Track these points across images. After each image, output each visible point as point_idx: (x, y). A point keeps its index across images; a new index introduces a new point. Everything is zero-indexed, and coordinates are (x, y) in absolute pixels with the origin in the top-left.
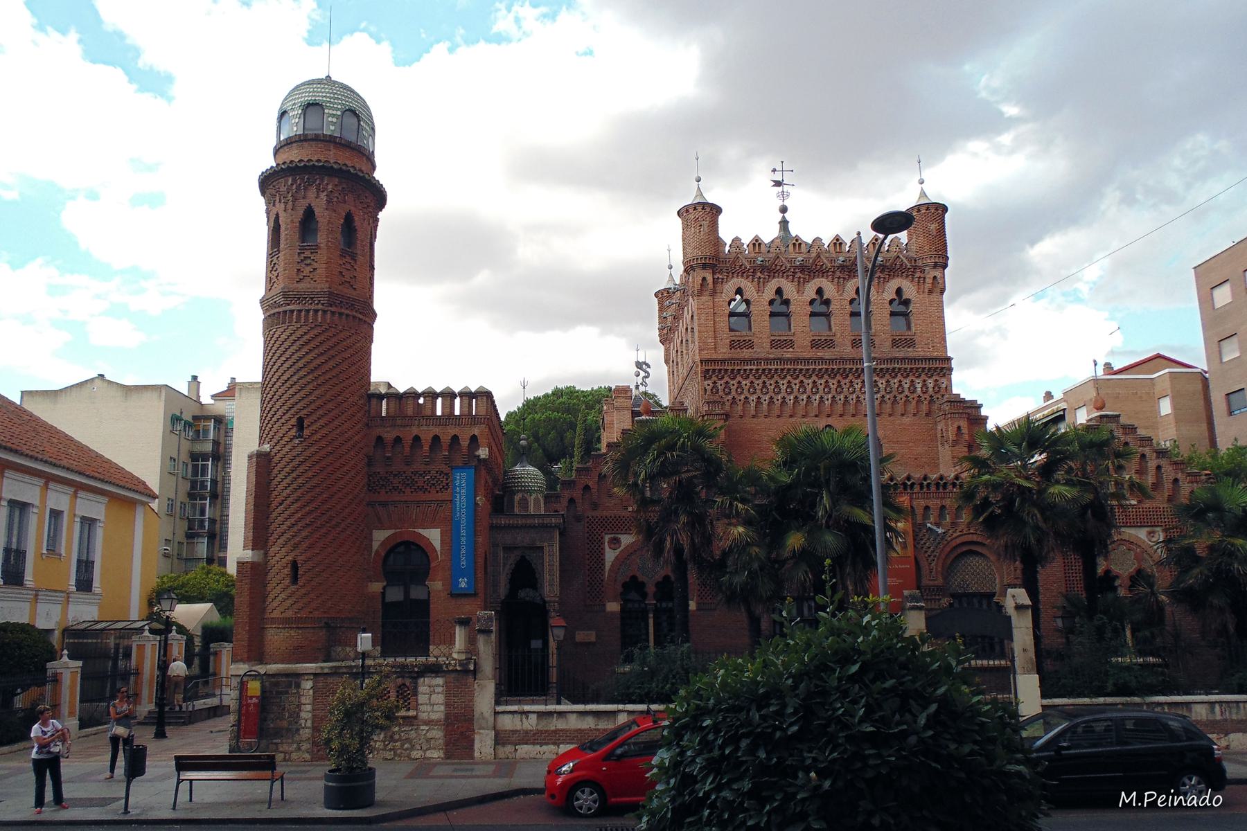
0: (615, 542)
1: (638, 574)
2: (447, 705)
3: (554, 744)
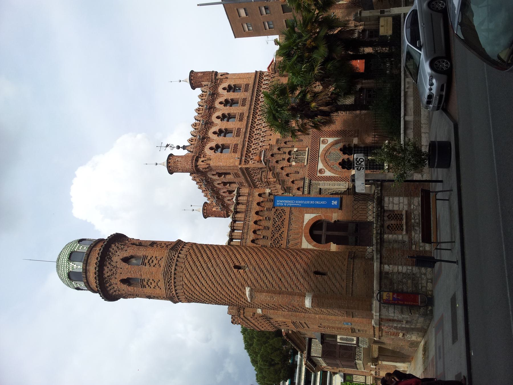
0: (321, 171)
2: (399, 196)
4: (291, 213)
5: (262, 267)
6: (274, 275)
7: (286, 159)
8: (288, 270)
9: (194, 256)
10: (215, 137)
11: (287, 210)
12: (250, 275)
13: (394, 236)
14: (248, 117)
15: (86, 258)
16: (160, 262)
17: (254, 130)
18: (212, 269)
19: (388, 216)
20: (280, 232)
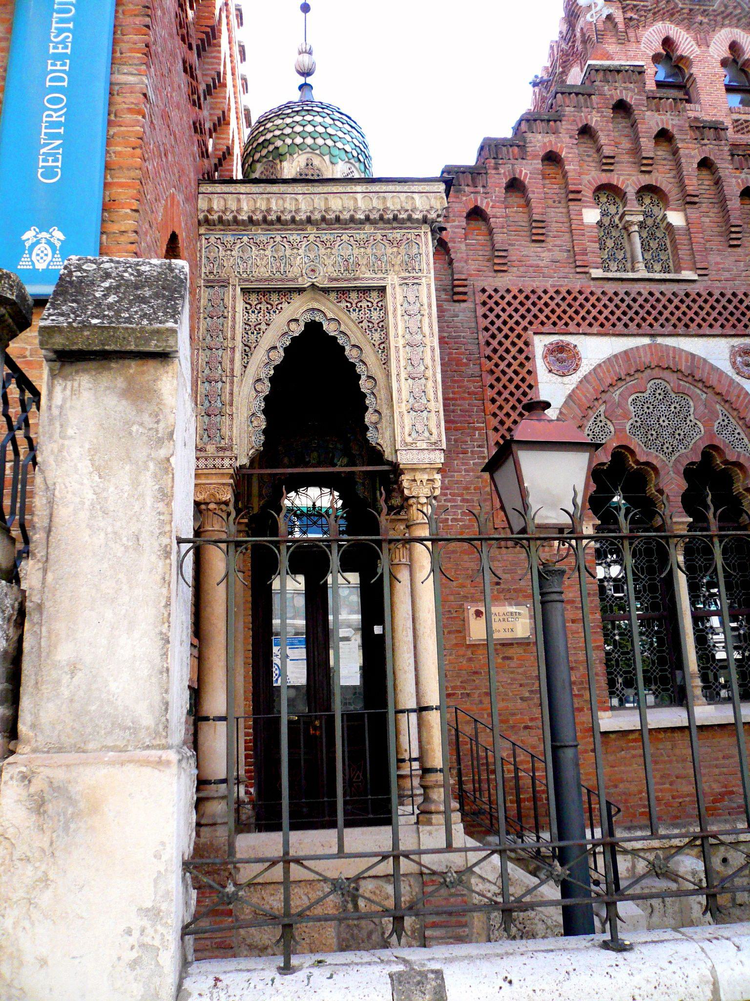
0: (563, 358)
1: (635, 443)
10: (718, 48)
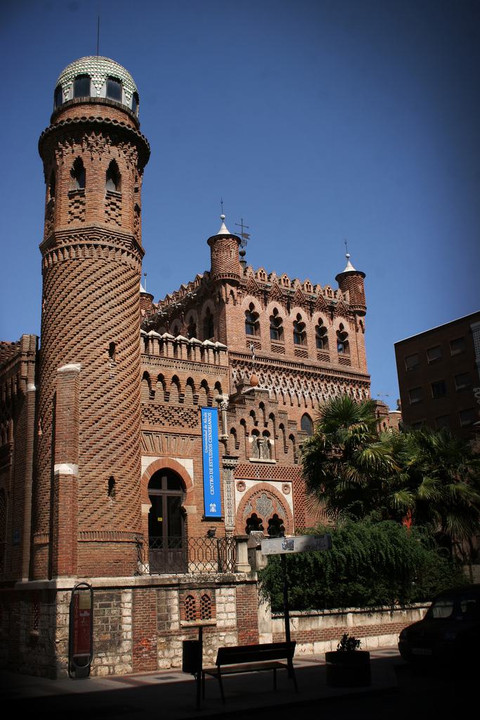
2: (238, 612)
3: (310, 642)
4: (193, 436)
5: (115, 390)
6: (103, 410)
7: (257, 428)
8: (113, 434)
9: (125, 276)
10: (269, 311)
11: (197, 430)
12: (101, 369)
13: (177, 607)
14: (302, 365)
15: (113, 104)
16: (112, 221)
17: (284, 375)
18: (107, 306)
19: (205, 595)
20: (162, 419)
